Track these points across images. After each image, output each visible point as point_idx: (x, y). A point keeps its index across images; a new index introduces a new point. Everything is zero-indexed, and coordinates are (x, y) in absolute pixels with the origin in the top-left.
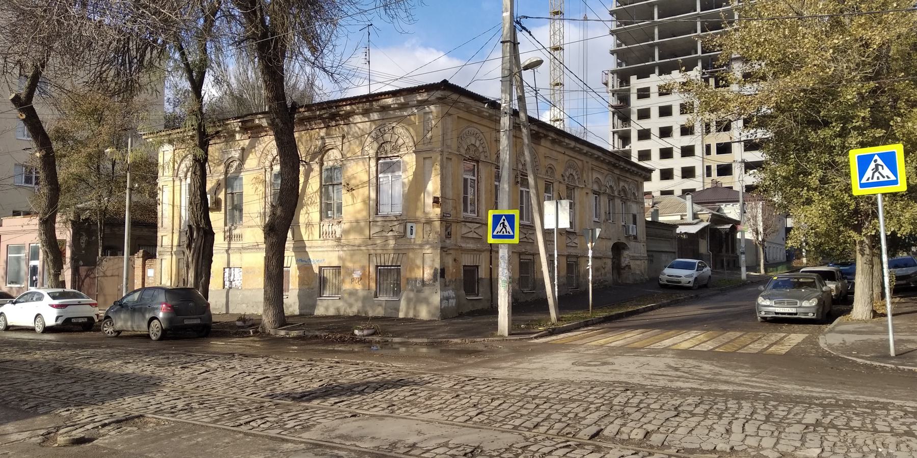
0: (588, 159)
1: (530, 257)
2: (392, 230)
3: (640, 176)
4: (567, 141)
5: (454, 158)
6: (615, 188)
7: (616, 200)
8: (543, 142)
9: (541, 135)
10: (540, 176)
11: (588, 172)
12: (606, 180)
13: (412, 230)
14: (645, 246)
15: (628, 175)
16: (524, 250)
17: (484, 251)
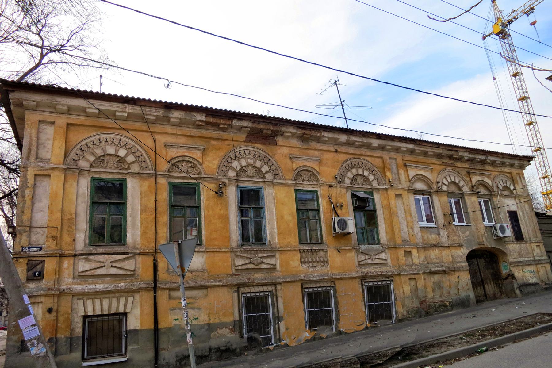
0: (393, 155)
1: (270, 288)
3: (512, 165)
4: (326, 135)
5: (404, 194)
6: (462, 184)
7: (466, 198)
8: (280, 140)
10: (280, 181)
11: (398, 170)
15: (488, 167)
17: (138, 290)
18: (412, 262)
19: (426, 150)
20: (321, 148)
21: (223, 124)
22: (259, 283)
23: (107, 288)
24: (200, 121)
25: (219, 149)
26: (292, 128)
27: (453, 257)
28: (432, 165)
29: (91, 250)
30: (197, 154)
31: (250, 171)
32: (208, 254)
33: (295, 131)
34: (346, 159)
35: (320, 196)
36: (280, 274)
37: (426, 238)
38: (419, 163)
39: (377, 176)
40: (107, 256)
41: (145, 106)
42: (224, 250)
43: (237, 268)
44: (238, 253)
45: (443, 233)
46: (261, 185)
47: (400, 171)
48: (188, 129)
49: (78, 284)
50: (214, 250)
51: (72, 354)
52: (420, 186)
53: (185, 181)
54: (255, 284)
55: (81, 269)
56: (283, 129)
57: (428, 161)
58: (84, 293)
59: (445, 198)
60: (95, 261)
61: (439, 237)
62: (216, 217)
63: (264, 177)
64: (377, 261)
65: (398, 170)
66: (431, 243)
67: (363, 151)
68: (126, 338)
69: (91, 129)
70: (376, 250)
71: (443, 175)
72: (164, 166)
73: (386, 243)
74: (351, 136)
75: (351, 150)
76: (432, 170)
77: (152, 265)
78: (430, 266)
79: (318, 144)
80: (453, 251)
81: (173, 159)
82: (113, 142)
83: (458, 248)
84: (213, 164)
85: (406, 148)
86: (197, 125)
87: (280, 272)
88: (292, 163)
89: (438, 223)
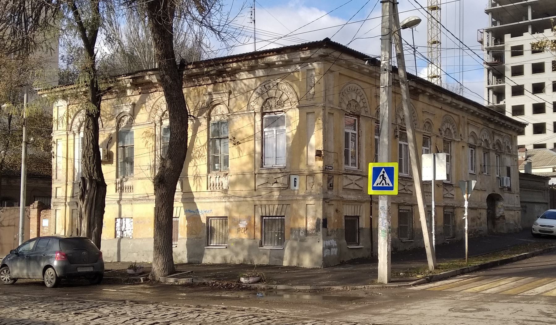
0: (464, 114)
1: (409, 208)
2: (276, 182)
3: (514, 130)
4: (444, 96)
5: (336, 113)
6: (490, 142)
8: (421, 97)
9: (419, 91)
10: (419, 130)
11: (464, 127)
12: (482, 133)
13: (295, 182)
14: (519, 197)
15: (502, 129)
16: (402, 201)
17: (364, 202)
28: (478, 124)
38: (473, 122)
75: (448, 109)
85: (473, 110)
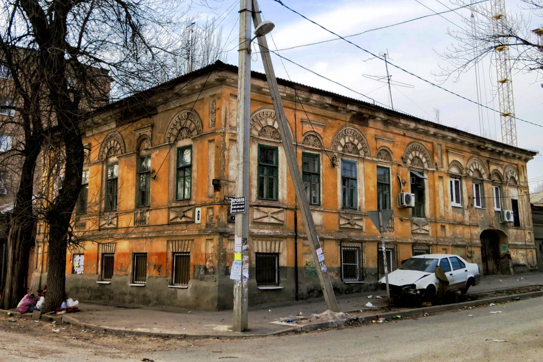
0: (440, 141)
1: (359, 245)
2: (184, 216)
3: (520, 158)
4: (403, 121)
6: (483, 171)
7: (485, 184)
8: (371, 123)
9: (365, 115)
10: (369, 158)
11: (442, 155)
12: (470, 163)
13: (198, 215)
14: (532, 235)
15: (502, 158)
16: (346, 237)
17: (285, 238)
18: (445, 236)
19: (464, 140)
20: (396, 131)
21: (341, 107)
22: (354, 240)
23: (271, 233)
24: (327, 104)
25: (333, 127)
26: (382, 114)
27: (471, 234)
28: (464, 152)
29: (260, 203)
30: (320, 131)
31: (350, 147)
32: (324, 214)
33: (383, 117)
34: (409, 142)
35: (391, 172)
36: (365, 234)
37: (455, 216)
38: (456, 150)
39: (428, 159)
40: (269, 209)
41: (298, 89)
42: (334, 211)
43: (341, 226)
44: (341, 215)
45: (467, 213)
46: (356, 160)
47: (443, 157)
48: (317, 109)
49: (254, 228)
50: (329, 211)
51: (251, 280)
52: (454, 170)
53: (312, 152)
54: (351, 240)
55: (255, 217)
56: (377, 114)
57: (461, 149)
58: (258, 235)
59: (470, 183)
60: (263, 212)
61: (463, 217)
62: (330, 184)
63: (358, 154)
64: (423, 232)
65: (442, 155)
66: (457, 221)
67: (421, 137)
68: (278, 272)
69: (258, 103)
70: (423, 222)
71: (470, 162)
72: (300, 139)
73: (429, 217)
74: (418, 124)
75: (414, 135)
76: (463, 157)
77: (294, 219)
78: (457, 240)
79: (394, 128)
80: (472, 229)
81: (306, 133)
82: (271, 115)
83: (476, 227)
84: (329, 140)
85: (451, 137)
86: (323, 106)
87: (365, 232)
88: (376, 143)
89: (464, 204)
